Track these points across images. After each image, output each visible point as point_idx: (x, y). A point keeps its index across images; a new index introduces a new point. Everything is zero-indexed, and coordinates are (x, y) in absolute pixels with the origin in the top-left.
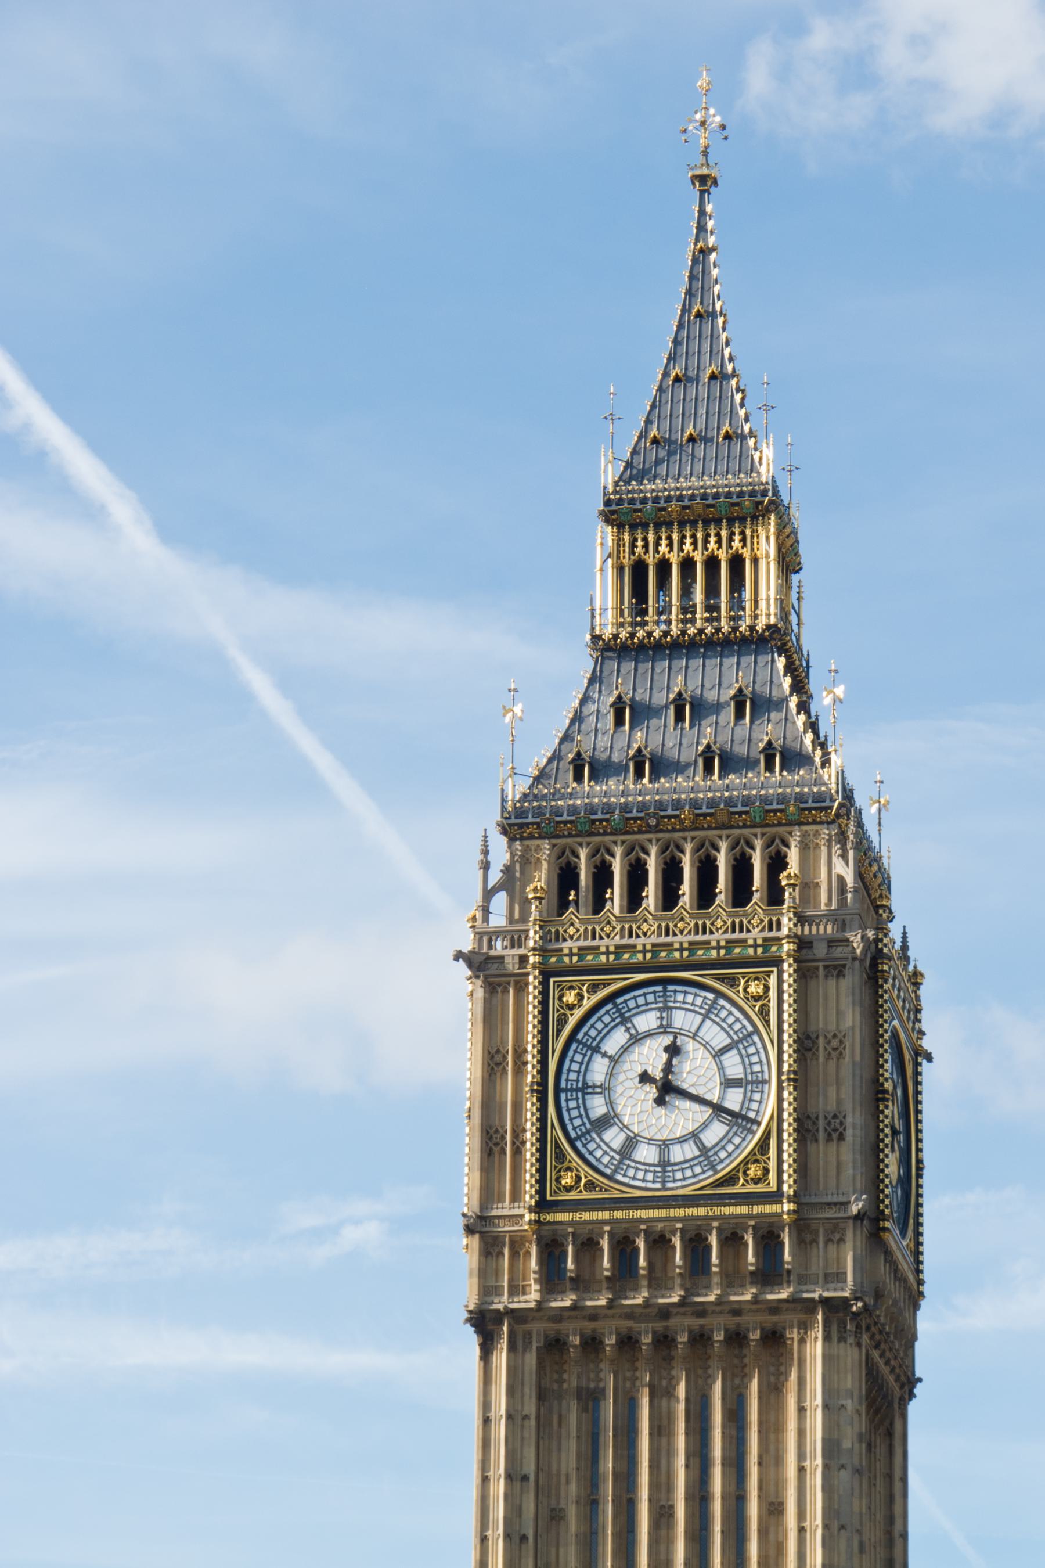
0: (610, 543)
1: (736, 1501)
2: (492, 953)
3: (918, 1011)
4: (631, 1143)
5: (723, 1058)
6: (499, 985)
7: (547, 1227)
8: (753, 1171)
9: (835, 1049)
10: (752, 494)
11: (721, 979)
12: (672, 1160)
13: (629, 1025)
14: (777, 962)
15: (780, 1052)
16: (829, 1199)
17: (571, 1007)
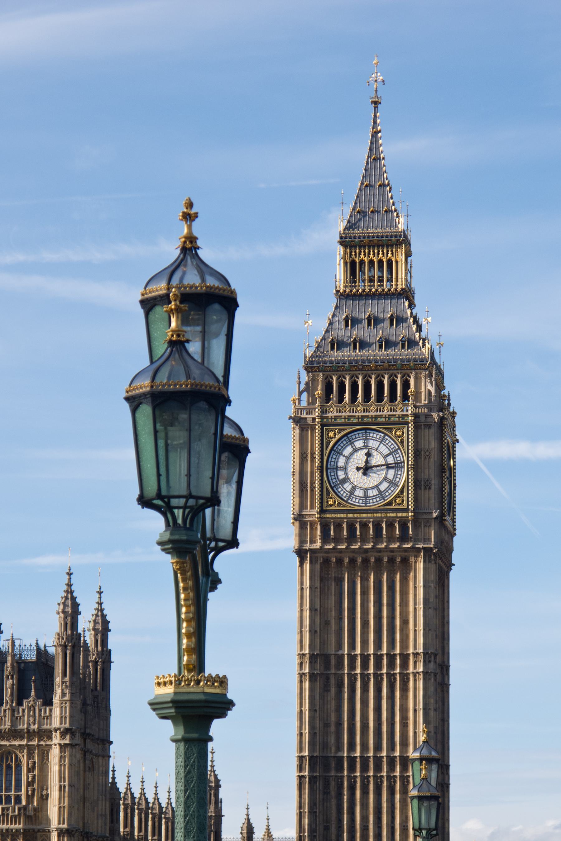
0: (342, 253)
1: (391, 618)
2: (302, 416)
3: (454, 427)
4: (354, 488)
5: (387, 458)
6: (305, 428)
7: (323, 520)
8: (398, 500)
9: (427, 456)
10: (396, 236)
11: (386, 429)
12: (369, 496)
13: (353, 445)
14: (407, 423)
15: (408, 457)
16: (426, 511)
17: (332, 438)
